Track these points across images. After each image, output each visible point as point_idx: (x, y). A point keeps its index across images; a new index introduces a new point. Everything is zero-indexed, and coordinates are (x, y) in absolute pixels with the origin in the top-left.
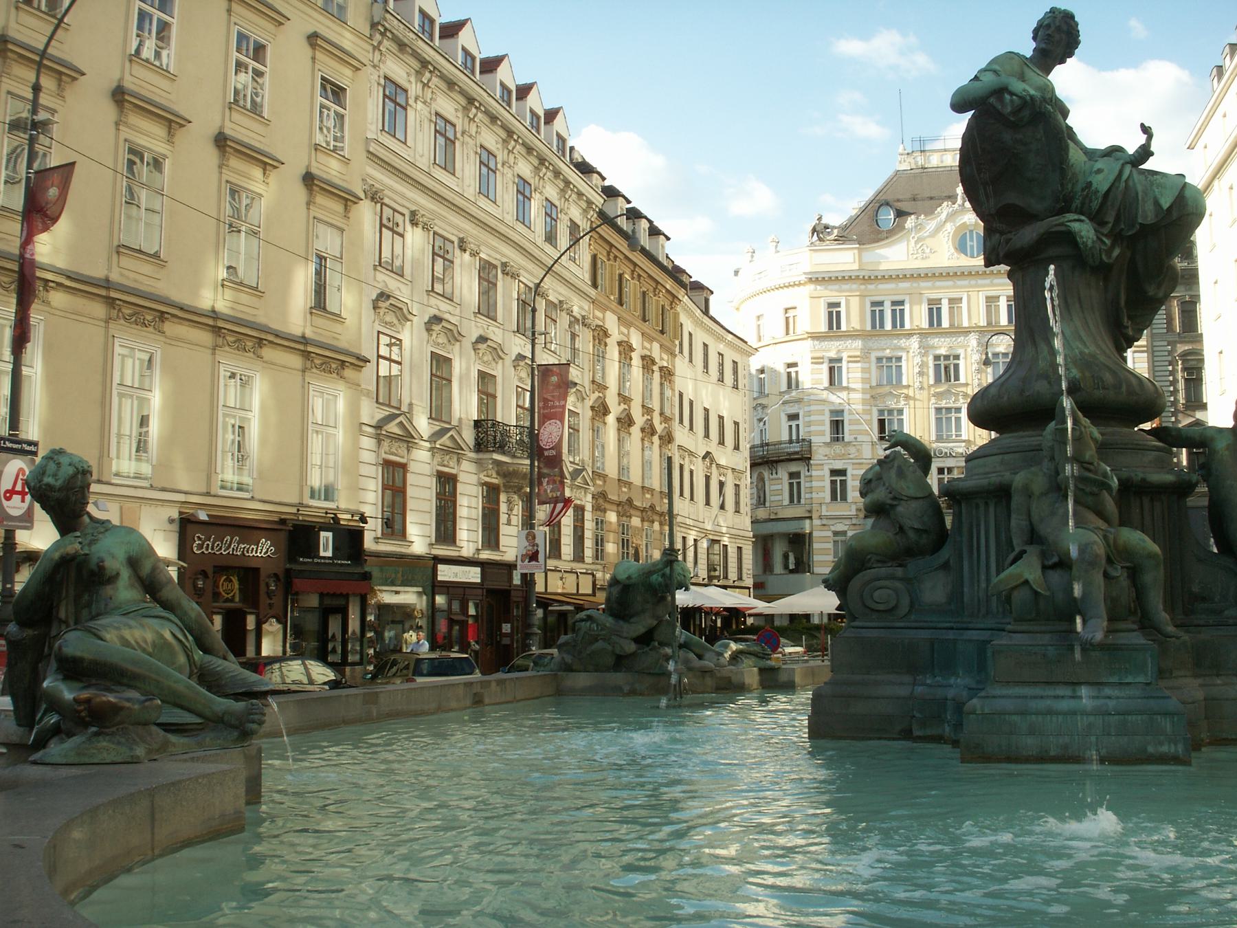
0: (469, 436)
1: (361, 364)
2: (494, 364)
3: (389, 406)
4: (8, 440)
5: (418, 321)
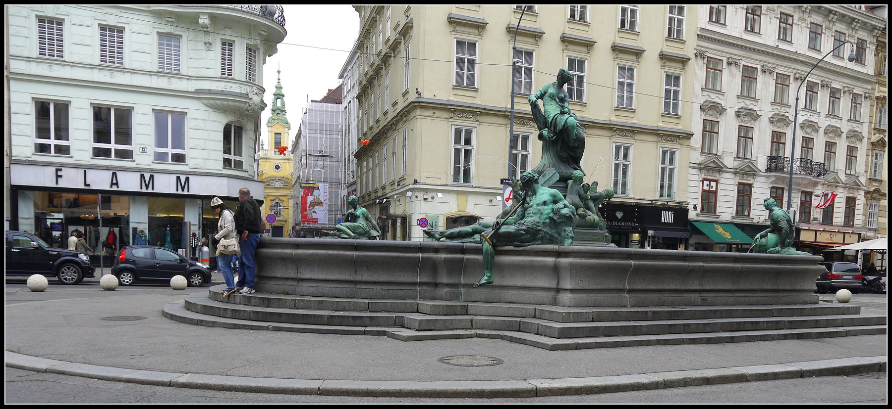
0: (762, 164)
1: (690, 136)
2: (785, 127)
3: (710, 154)
4: (507, 180)
5: (731, 113)
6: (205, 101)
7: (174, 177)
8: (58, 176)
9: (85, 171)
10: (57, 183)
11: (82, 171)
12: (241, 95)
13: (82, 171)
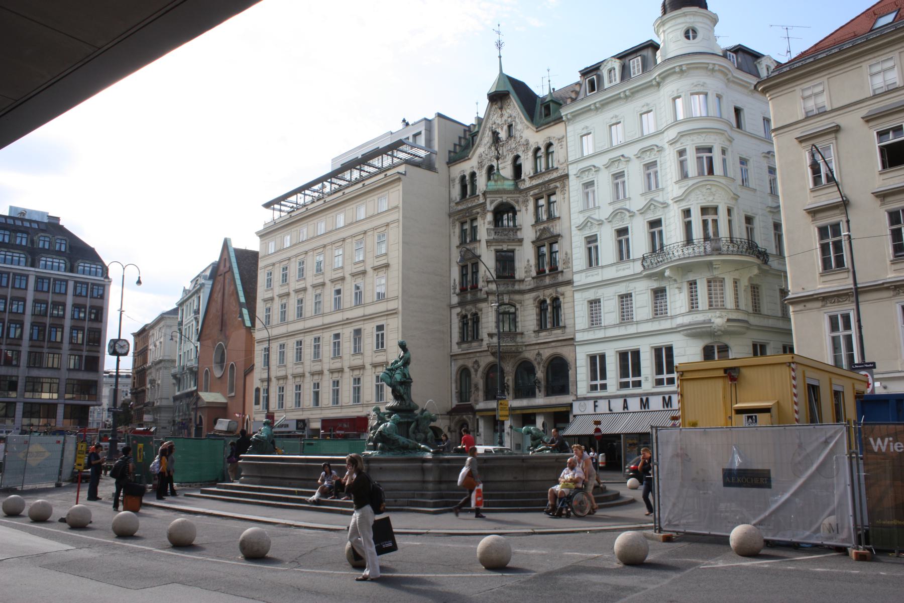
6: (682, 333)
7: (661, 397)
8: (595, 406)
9: (609, 401)
10: (595, 411)
11: (607, 401)
12: (704, 322)
13: (607, 401)
